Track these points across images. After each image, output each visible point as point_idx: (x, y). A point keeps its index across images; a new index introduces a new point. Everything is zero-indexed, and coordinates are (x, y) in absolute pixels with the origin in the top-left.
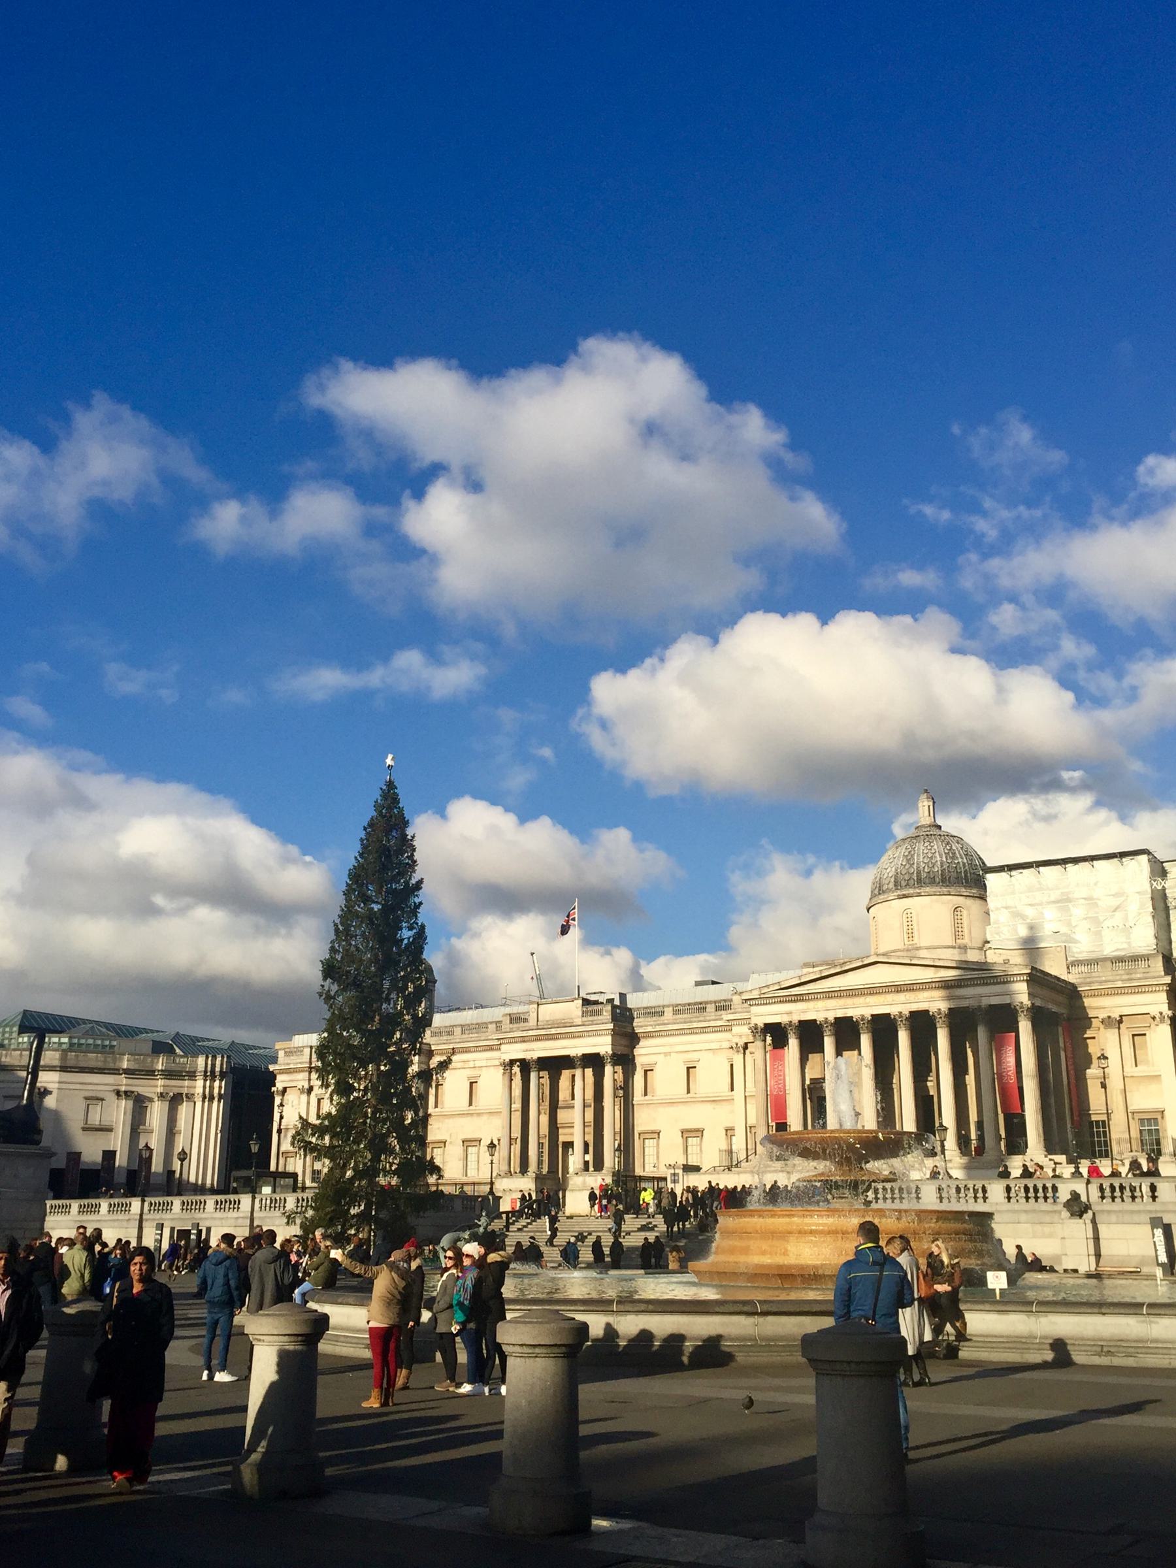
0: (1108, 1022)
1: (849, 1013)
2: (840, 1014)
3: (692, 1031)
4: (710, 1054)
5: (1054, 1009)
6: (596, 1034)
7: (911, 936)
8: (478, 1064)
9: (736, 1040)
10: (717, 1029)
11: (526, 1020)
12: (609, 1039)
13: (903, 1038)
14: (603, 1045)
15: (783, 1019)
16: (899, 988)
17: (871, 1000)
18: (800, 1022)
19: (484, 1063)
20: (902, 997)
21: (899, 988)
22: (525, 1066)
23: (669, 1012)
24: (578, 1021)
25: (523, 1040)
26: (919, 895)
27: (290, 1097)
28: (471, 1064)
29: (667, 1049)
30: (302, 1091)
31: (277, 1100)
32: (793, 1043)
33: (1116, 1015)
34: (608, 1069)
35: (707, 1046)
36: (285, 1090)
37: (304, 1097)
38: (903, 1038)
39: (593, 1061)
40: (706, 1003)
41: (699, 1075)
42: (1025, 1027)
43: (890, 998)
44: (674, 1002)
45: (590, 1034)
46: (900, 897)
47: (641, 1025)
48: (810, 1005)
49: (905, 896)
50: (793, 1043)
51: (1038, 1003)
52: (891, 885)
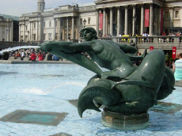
0: (171, 8)
2: (114, 6)
4: (93, 16)
5: (159, 5)
6: (71, 12)
8: (51, 19)
11: (58, 10)
12: (73, 13)
13: (126, 11)
14: (72, 15)
18: (106, 8)
22: (58, 18)
24: (67, 10)
25: (57, 14)
27: (22, 26)
30: (23, 25)
31: (20, 26)
32: (104, 12)
33: (173, 6)
34: (73, 19)
36: (21, 25)
37: (24, 26)
38: (126, 11)
39: (70, 18)
40: (93, 6)
41: (91, 20)
42: (151, 8)
44: (87, 6)
47: (81, 10)
48: (108, 4)
50: (104, 12)
51: (155, 3)
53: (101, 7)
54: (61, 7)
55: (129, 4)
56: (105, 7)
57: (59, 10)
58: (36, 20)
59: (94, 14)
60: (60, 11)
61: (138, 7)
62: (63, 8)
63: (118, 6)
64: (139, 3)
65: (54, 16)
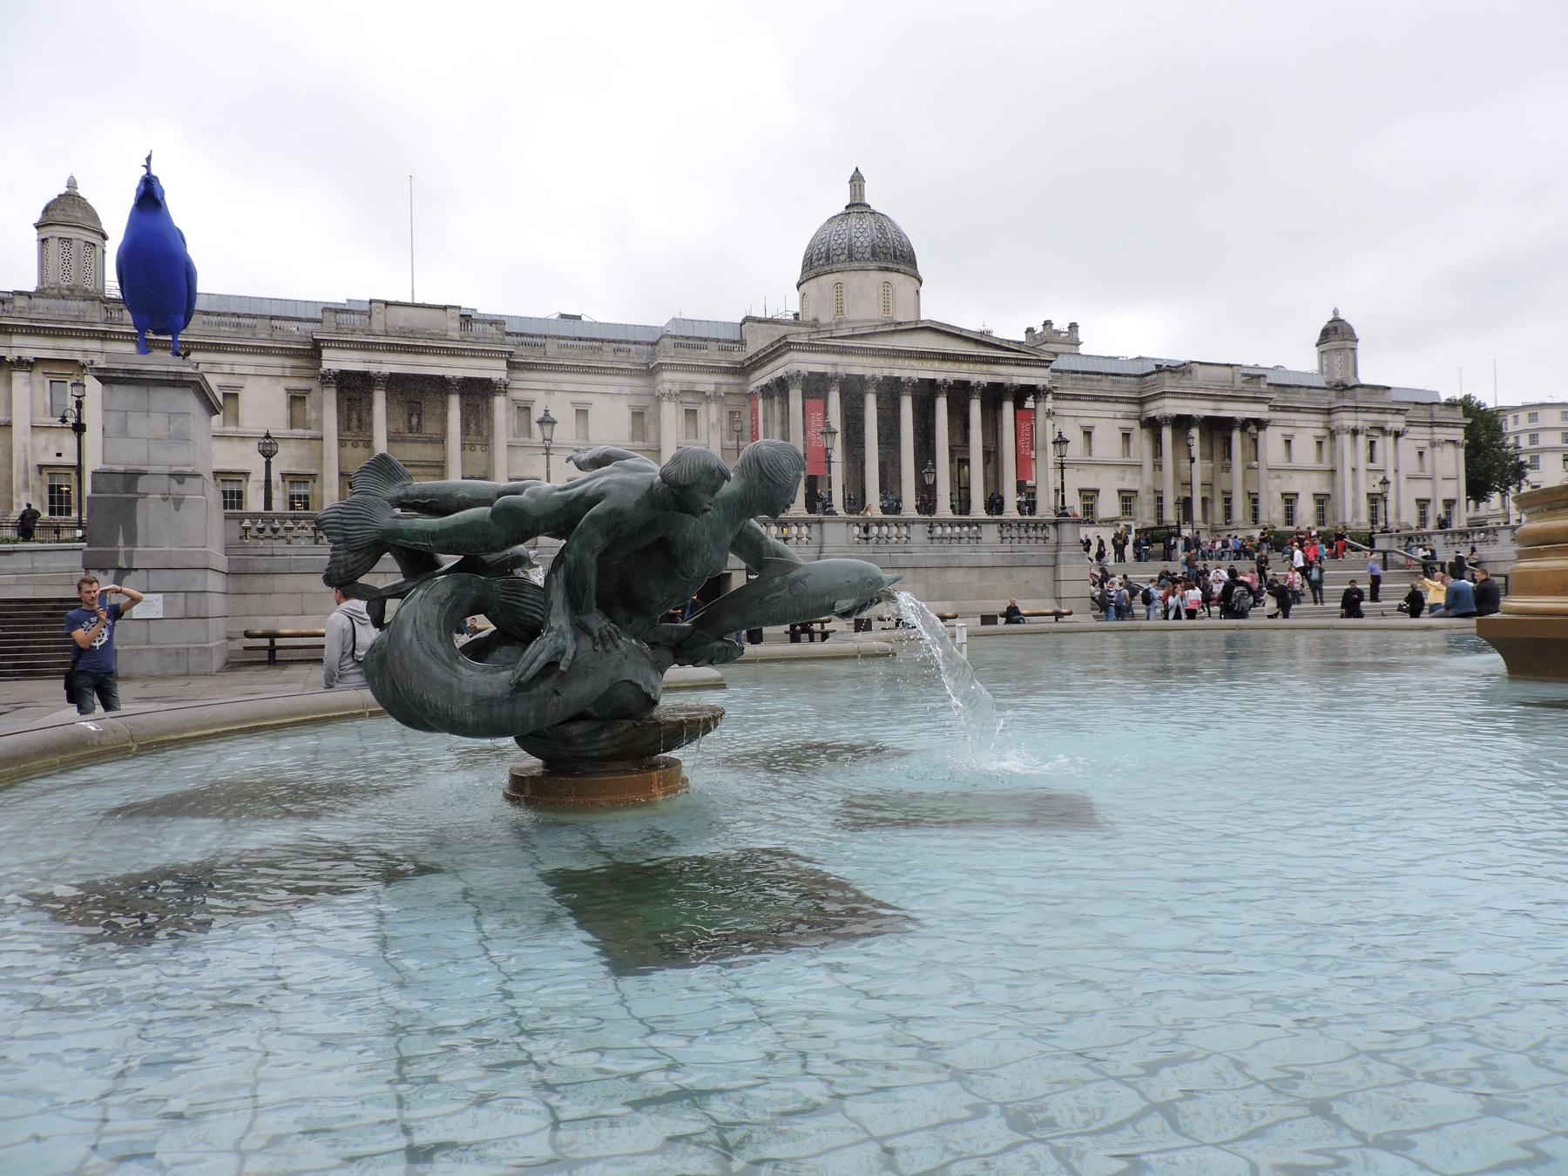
1: (897, 373)
2: (886, 373)
3: (588, 370)
4: (606, 399)
7: (886, 309)
8: (237, 370)
9: (667, 386)
10: (618, 372)
13: (942, 404)
15: (830, 370)
16: (945, 357)
17: (915, 364)
19: (251, 370)
20: (948, 366)
21: (945, 357)
23: (551, 347)
24: (456, 335)
25: (364, 347)
26: (898, 271)
28: (226, 369)
29: (551, 386)
34: (499, 402)
35: (602, 389)
38: (942, 404)
40: (603, 341)
43: (936, 364)
45: (474, 353)
46: (881, 269)
49: (887, 269)
50: (834, 398)
52: (867, 255)
53: (820, 369)
54: (387, 304)
55: (957, 376)
56: (840, 370)
57: (377, 326)
58: (78, 356)
59: (611, 390)
60: (387, 334)
61: (994, 396)
62: (400, 318)
63: (910, 379)
64: (998, 380)
65: (326, 353)
